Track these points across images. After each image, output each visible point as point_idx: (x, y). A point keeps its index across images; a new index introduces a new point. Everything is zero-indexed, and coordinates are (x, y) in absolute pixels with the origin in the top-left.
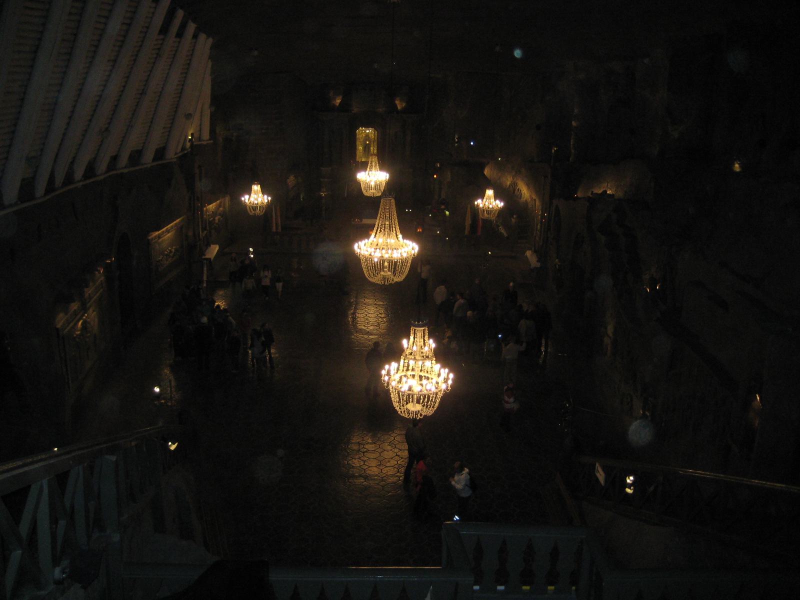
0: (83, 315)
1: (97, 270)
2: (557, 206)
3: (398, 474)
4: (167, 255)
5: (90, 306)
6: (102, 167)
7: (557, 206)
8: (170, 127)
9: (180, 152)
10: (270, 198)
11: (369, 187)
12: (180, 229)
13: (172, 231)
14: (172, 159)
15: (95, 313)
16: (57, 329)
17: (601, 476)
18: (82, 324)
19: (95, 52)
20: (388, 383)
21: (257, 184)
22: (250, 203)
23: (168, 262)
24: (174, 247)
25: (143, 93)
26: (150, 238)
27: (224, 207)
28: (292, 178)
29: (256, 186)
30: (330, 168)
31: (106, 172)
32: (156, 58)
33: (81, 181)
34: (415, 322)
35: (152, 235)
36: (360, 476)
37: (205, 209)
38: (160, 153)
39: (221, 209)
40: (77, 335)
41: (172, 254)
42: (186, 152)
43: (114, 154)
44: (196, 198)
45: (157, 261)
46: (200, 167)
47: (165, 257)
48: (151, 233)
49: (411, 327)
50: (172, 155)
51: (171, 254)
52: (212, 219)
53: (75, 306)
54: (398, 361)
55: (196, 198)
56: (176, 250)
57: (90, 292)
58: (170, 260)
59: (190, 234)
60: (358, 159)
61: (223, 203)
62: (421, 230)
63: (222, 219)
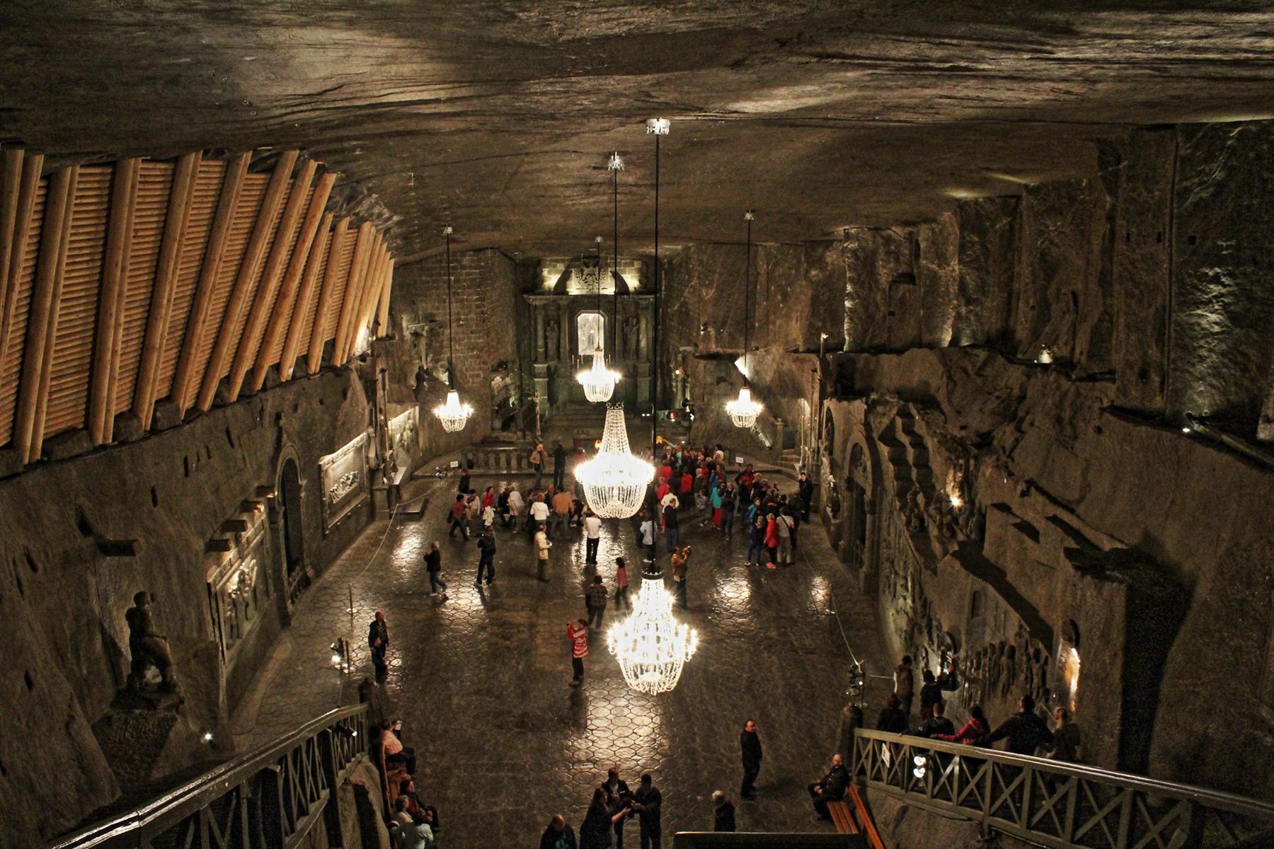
0: (241, 564)
2: (829, 409)
3: (636, 757)
7: (828, 409)
12: (358, 450)
15: (254, 561)
16: (209, 585)
17: (886, 756)
18: (240, 577)
27: (414, 417)
28: (498, 379)
36: (588, 761)
37: (389, 423)
46: (383, 371)
51: (349, 482)
53: (230, 555)
58: (348, 489)
59: (372, 455)
60: (581, 353)
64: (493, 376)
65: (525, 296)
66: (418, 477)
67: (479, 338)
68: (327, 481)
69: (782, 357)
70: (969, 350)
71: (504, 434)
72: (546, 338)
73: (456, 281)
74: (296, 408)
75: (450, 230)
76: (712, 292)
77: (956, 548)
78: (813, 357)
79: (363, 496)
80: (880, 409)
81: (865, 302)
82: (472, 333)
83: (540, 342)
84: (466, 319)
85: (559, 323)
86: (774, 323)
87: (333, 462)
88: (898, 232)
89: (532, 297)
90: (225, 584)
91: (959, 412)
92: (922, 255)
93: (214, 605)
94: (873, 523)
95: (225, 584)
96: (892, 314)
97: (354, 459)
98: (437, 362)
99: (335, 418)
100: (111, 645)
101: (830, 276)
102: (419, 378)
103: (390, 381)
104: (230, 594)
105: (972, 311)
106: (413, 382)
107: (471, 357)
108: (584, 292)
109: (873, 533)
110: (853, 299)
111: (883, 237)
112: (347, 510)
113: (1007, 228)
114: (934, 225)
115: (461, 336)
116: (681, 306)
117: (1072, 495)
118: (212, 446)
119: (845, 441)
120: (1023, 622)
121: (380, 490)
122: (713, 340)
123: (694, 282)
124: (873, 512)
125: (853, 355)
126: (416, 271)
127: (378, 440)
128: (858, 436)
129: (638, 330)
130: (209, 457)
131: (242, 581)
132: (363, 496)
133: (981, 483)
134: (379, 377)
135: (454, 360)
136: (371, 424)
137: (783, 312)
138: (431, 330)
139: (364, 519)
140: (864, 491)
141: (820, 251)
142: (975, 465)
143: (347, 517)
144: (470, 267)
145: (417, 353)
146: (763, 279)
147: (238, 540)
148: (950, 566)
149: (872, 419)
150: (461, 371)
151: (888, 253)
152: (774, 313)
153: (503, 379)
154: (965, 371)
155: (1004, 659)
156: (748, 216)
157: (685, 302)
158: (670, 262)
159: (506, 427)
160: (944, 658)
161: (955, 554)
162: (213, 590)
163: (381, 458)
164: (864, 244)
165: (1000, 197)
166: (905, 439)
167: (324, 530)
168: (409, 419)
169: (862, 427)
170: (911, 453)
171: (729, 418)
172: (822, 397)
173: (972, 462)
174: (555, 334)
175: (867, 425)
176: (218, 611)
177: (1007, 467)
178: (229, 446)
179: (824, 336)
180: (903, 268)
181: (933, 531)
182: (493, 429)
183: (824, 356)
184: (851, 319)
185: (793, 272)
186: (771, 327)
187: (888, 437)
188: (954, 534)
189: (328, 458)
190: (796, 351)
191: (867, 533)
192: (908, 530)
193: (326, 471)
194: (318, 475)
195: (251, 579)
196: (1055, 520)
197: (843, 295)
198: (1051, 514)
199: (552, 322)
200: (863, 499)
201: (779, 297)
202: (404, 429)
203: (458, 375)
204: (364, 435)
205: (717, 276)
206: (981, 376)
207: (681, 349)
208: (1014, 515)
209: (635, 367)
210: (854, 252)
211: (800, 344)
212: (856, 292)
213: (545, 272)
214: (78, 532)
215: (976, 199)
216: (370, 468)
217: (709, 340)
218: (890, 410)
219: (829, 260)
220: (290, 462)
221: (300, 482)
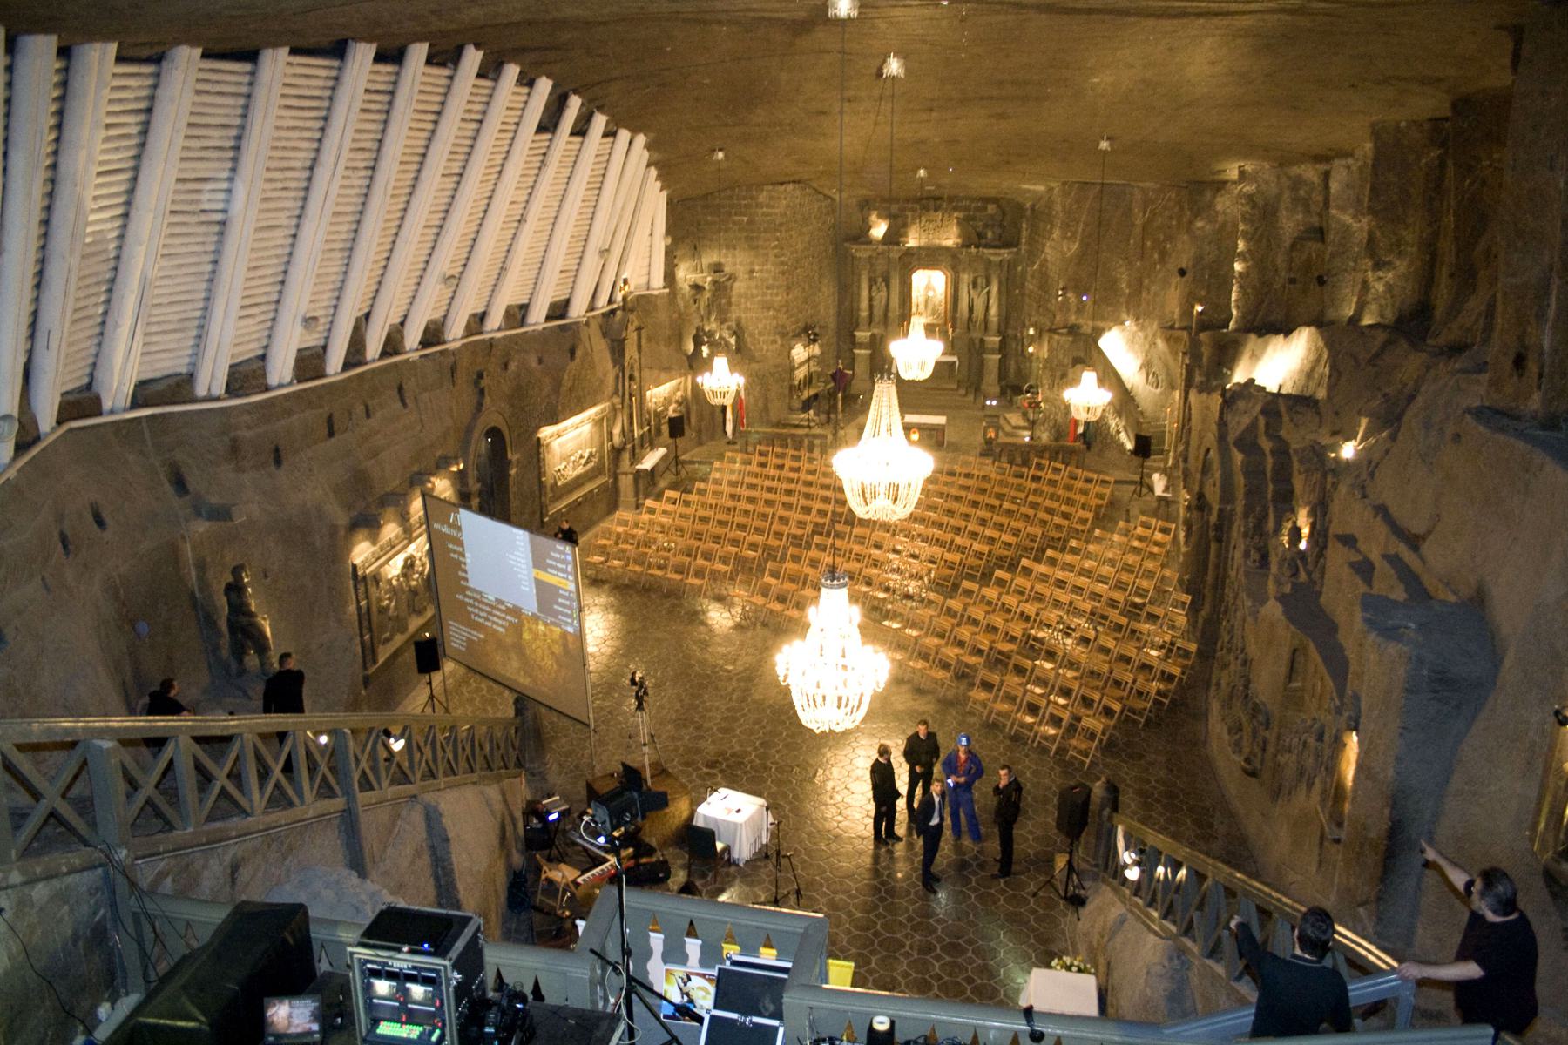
5: (421, 535)
6: (455, 331)
8: (577, 270)
12: (598, 423)
16: (355, 567)
19: (422, 163)
20: (786, 677)
24: (588, 451)
25: (521, 221)
27: (686, 390)
31: (462, 338)
32: (540, 168)
37: (648, 393)
38: (559, 310)
42: (615, 306)
43: (480, 310)
46: (639, 329)
48: (543, 429)
50: (577, 311)
51: (583, 461)
53: (391, 530)
56: (591, 455)
58: (580, 470)
59: (617, 431)
64: (793, 343)
65: (847, 245)
67: (777, 295)
68: (548, 457)
69: (1154, 335)
70: (1366, 331)
72: (871, 299)
73: (751, 222)
74: (506, 366)
75: (720, 155)
76: (1075, 247)
77: (1287, 589)
78: (1185, 334)
79: (599, 481)
80: (1241, 405)
81: (1259, 261)
82: (768, 288)
83: (864, 304)
84: (761, 271)
85: (887, 281)
86: (1149, 290)
88: (1310, 173)
89: (855, 247)
90: (382, 565)
91: (1337, 413)
92: (1332, 204)
93: (362, 589)
94: (1218, 556)
95: (382, 565)
96: (1292, 281)
98: (722, 323)
99: (557, 385)
100: (209, 620)
101: (1223, 226)
102: (698, 342)
103: (649, 340)
104: (389, 582)
105: (1380, 278)
106: (690, 347)
107: (766, 318)
108: (923, 242)
109: (1217, 567)
110: (1245, 260)
111: (1289, 178)
113: (1437, 163)
114: (1350, 161)
115: (754, 291)
116: (1042, 265)
117: (1417, 526)
118: (372, 403)
119: (1199, 447)
120: (1335, 694)
121: (626, 474)
122: (1073, 309)
123: (1057, 233)
124: (1219, 540)
125: (1236, 334)
126: (699, 209)
127: (626, 411)
128: (1211, 438)
129: (988, 293)
130: (368, 415)
131: (409, 565)
132: (599, 481)
133: (1335, 507)
134: (632, 336)
135: (743, 321)
136: (616, 392)
137: (1160, 276)
138: (714, 282)
139: (602, 507)
140: (1210, 509)
141: (1208, 195)
142: (1333, 483)
144: (768, 206)
145: (698, 308)
146: (1137, 231)
147: (404, 518)
148: (1273, 609)
149: (1229, 417)
150: (752, 335)
151: (1295, 200)
152: (1149, 276)
154: (1356, 359)
155: (1311, 741)
156: (1104, 145)
157: (1046, 260)
158: (1033, 208)
159: (806, 406)
160: (1255, 733)
161: (1282, 599)
162: (360, 573)
163: (627, 433)
164: (1264, 187)
165: (1430, 120)
166: (1266, 445)
167: (542, 516)
168: (678, 389)
169: (1214, 427)
170: (1270, 461)
171: (1068, 407)
172: (1189, 384)
173: (1330, 479)
174: (884, 294)
175: (1222, 423)
176: (367, 597)
177: (1363, 487)
178: (399, 405)
179: (1199, 308)
180: (1315, 220)
181: (1274, 568)
183: (1197, 334)
184: (1241, 287)
185: (1174, 223)
186: (1144, 294)
187: (1247, 443)
188: (1295, 574)
189: (546, 432)
190: (1172, 327)
191: (1211, 567)
192: (1246, 564)
193: (548, 445)
194: (536, 450)
196: (1394, 560)
197: (1232, 255)
198: (1392, 552)
199: (880, 280)
200: (1208, 522)
201: (1156, 256)
202: (670, 404)
203: (749, 340)
204: (608, 404)
205: (1081, 225)
206: (1374, 365)
207: (1033, 319)
208: (1358, 551)
209: (982, 341)
210: (1250, 198)
211: (1176, 316)
212: (1249, 251)
213: (873, 217)
214: (168, 488)
215: (1398, 123)
216: (613, 447)
217: (1069, 310)
218: (1254, 405)
219: (1219, 207)
220: (494, 432)
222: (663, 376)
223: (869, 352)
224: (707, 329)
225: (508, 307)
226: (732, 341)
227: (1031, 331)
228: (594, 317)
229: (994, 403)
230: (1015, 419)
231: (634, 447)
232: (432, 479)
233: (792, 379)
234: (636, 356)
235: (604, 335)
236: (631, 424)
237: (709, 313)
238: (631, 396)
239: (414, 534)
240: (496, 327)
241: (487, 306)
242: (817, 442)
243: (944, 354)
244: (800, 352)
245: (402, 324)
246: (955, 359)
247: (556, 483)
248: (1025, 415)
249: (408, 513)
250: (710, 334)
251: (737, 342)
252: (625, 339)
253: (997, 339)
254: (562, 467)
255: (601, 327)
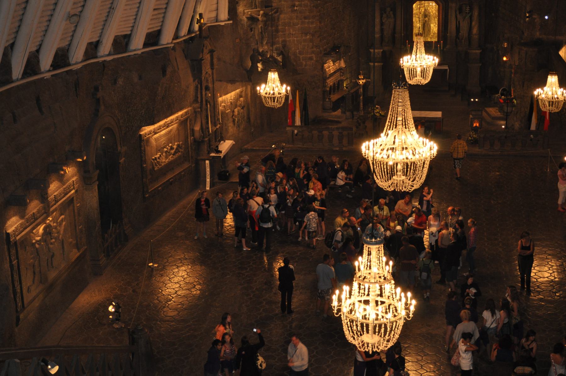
0: (46, 218)
1: (63, 170)
4: (166, 152)
9: (184, 36)
10: (289, 88)
11: (412, 72)
12: (183, 123)
13: (172, 125)
14: (168, 44)
15: (63, 217)
18: (45, 229)
21: (274, 71)
22: (266, 94)
23: (167, 160)
24: (176, 144)
26: (141, 133)
29: (272, 73)
30: (382, 50)
31: (83, 61)
33: (49, 71)
34: (367, 238)
35: (145, 130)
39: (242, 99)
40: (37, 241)
41: (174, 150)
42: (193, 35)
44: (204, 88)
45: (153, 159)
46: (211, 52)
47: (164, 154)
48: (143, 128)
49: (364, 245)
50: (167, 39)
51: (173, 151)
52: (229, 110)
54: (350, 284)
55: (204, 88)
56: (178, 146)
57: (55, 194)
58: (170, 158)
59: (197, 128)
61: (243, 94)
62: (478, 125)
63: (242, 110)
66: (247, 151)
68: (148, 149)
71: (336, 113)
74: (115, 82)
79: (186, 165)
87: (156, 133)
97: (178, 129)
106: (250, 64)
112: (169, 176)
127: (204, 113)
131: (48, 231)
134: (207, 57)
136: (196, 101)
143: (170, 183)
145: (254, 35)
147: (43, 197)
153: (334, 62)
159: (336, 105)
163: (204, 129)
168: (241, 96)
182: (324, 109)
189: (147, 130)
193: (148, 140)
195: (58, 232)
202: (236, 107)
204: (190, 108)
216: (194, 139)
221: (119, 148)
222: (229, 86)
223: (382, 64)
224: (261, 50)
225: (116, 36)
226: (279, 59)
227: (506, 45)
228: (178, 43)
229: (477, 100)
230: (493, 111)
231: (209, 140)
232: (64, 168)
233: (325, 86)
234: (210, 71)
235: (186, 57)
236: (207, 123)
237: (262, 38)
238: (206, 101)
239: (52, 209)
240: (107, 53)
241: (100, 36)
242: (345, 133)
243: (439, 64)
244: (330, 66)
245: (38, 51)
246: (446, 67)
247: (153, 168)
248: (501, 109)
249: (47, 194)
250: (263, 54)
251: (283, 59)
252: (202, 59)
253: (478, 52)
254: (159, 156)
255: (183, 51)
